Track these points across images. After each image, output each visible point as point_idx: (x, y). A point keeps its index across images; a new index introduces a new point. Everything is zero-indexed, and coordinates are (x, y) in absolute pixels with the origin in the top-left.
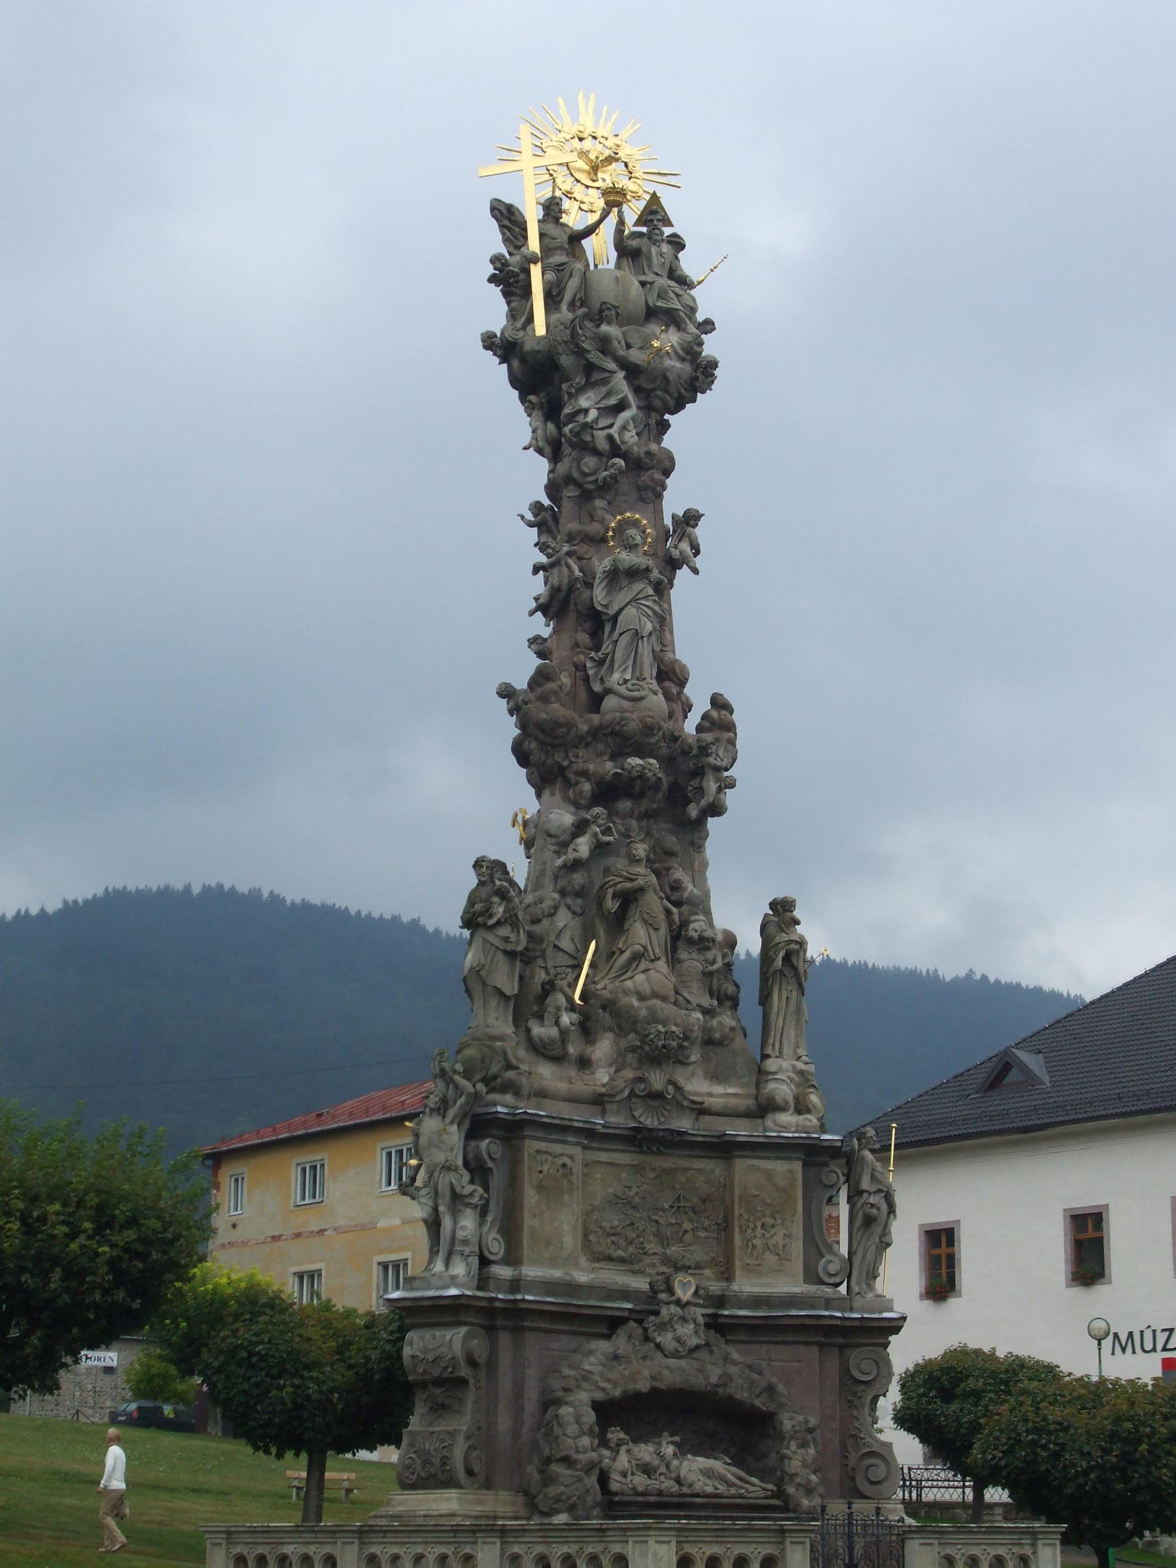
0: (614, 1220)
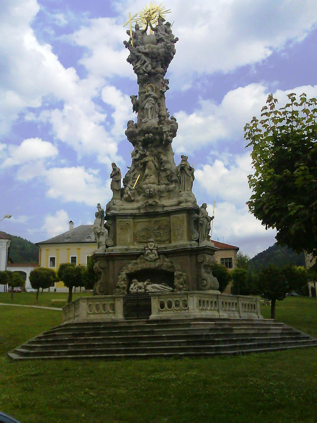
0: (144, 234)
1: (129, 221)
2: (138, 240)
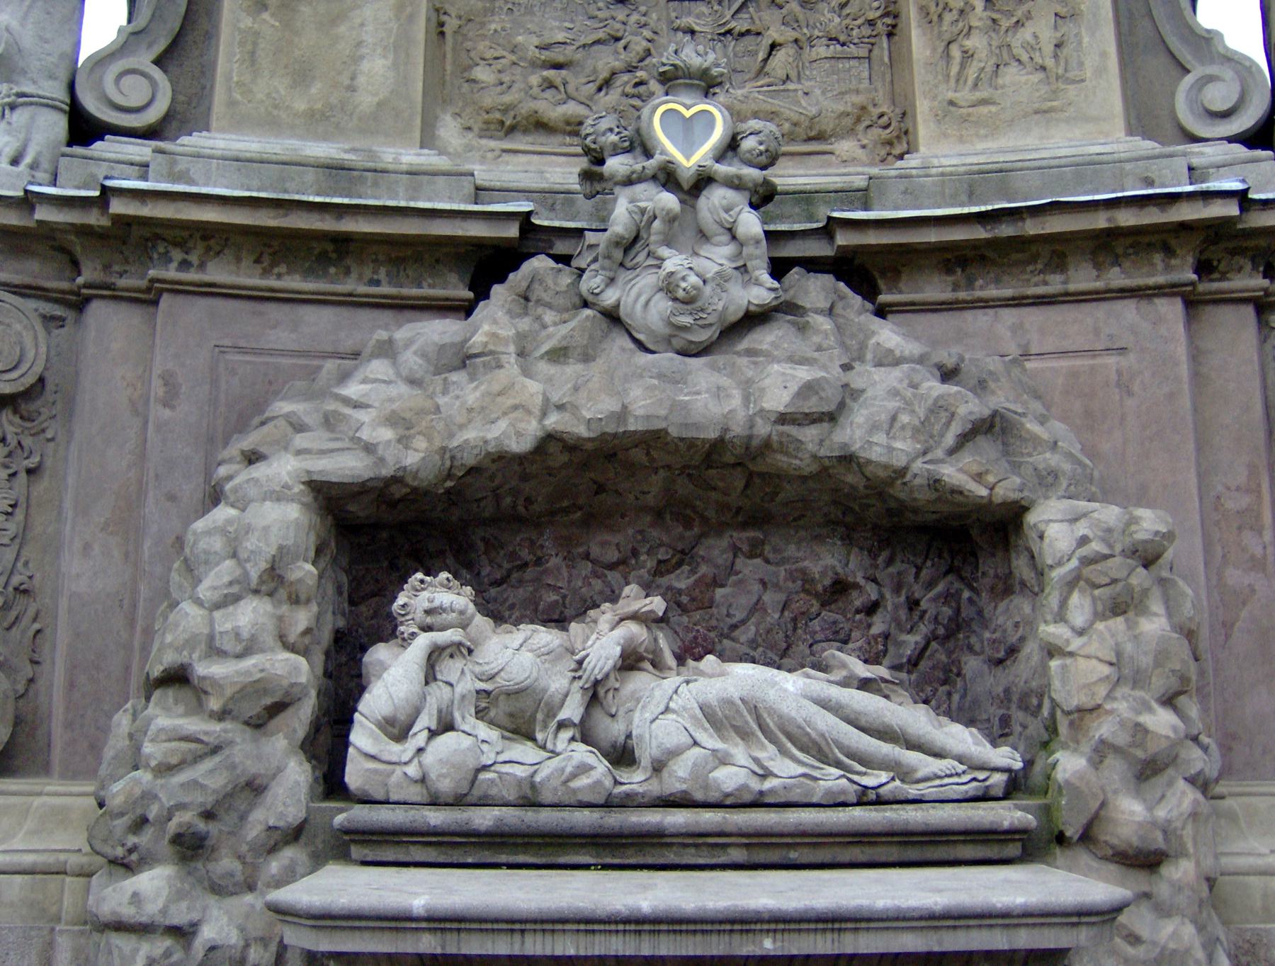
2: (488, 101)
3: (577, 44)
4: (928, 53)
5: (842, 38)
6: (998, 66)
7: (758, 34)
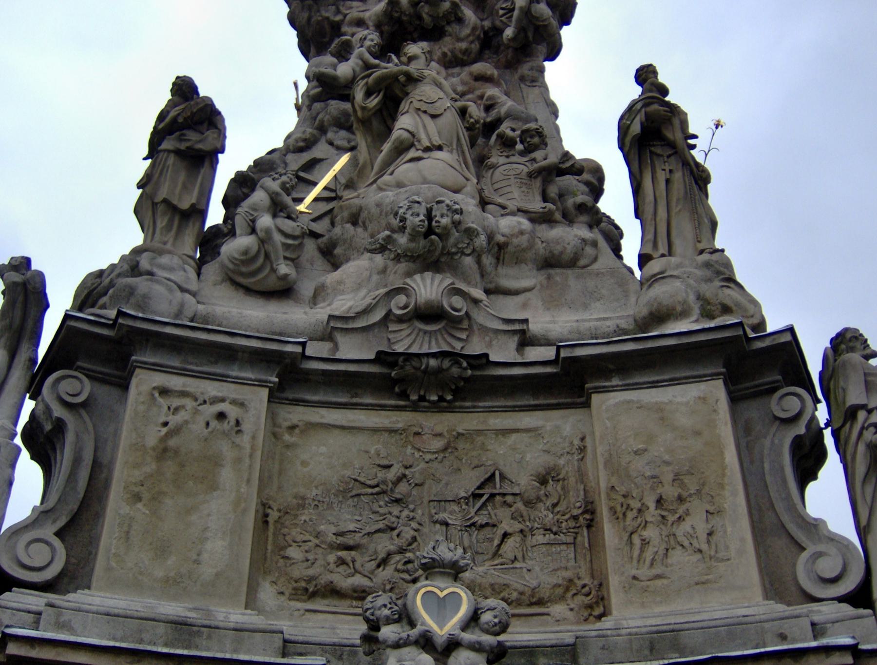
0: (348, 518)
1: (234, 402)
2: (297, 572)
3: (364, 532)
4: (616, 541)
5: (554, 529)
6: (667, 550)
7: (494, 526)
